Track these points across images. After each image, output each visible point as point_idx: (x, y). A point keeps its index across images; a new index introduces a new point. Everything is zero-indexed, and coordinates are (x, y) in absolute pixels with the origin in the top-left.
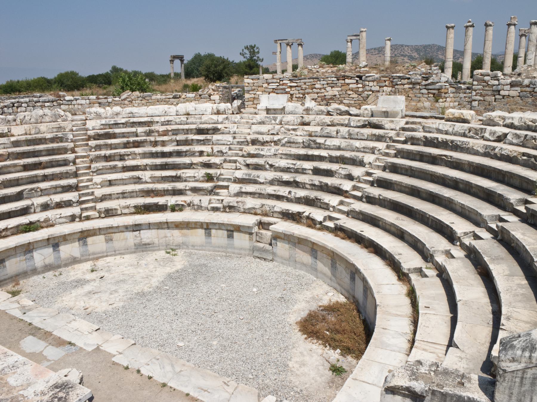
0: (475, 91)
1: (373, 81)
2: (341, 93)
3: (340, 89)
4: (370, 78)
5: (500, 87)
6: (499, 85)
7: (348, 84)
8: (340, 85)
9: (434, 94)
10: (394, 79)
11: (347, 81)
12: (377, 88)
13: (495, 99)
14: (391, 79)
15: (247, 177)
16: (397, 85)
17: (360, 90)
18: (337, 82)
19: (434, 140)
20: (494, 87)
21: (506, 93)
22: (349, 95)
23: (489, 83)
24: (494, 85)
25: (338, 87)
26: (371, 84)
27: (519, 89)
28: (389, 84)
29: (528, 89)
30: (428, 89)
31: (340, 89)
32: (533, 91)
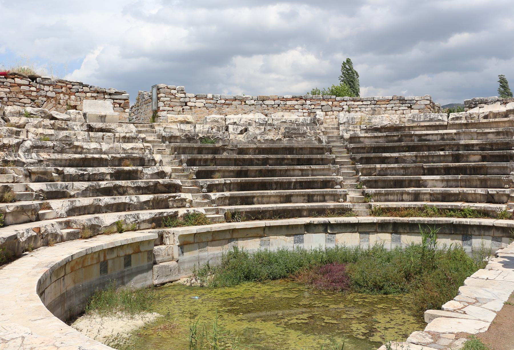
0: (164, 102)
1: (49, 85)
2: (8, 95)
3: (8, 90)
4: (46, 82)
5: (187, 100)
6: (186, 97)
7: (20, 85)
8: (9, 84)
9: (120, 104)
10: (73, 85)
11: (18, 81)
12: (53, 94)
13: (183, 109)
14: (68, 86)
15: (54, 190)
16: (77, 92)
17: (34, 94)
18: (5, 80)
19: (194, 137)
21: (193, 104)
22: (21, 99)
25: (6, 87)
26: (46, 88)
28: (67, 91)
29: (212, 101)
30: (114, 99)
31: (8, 90)
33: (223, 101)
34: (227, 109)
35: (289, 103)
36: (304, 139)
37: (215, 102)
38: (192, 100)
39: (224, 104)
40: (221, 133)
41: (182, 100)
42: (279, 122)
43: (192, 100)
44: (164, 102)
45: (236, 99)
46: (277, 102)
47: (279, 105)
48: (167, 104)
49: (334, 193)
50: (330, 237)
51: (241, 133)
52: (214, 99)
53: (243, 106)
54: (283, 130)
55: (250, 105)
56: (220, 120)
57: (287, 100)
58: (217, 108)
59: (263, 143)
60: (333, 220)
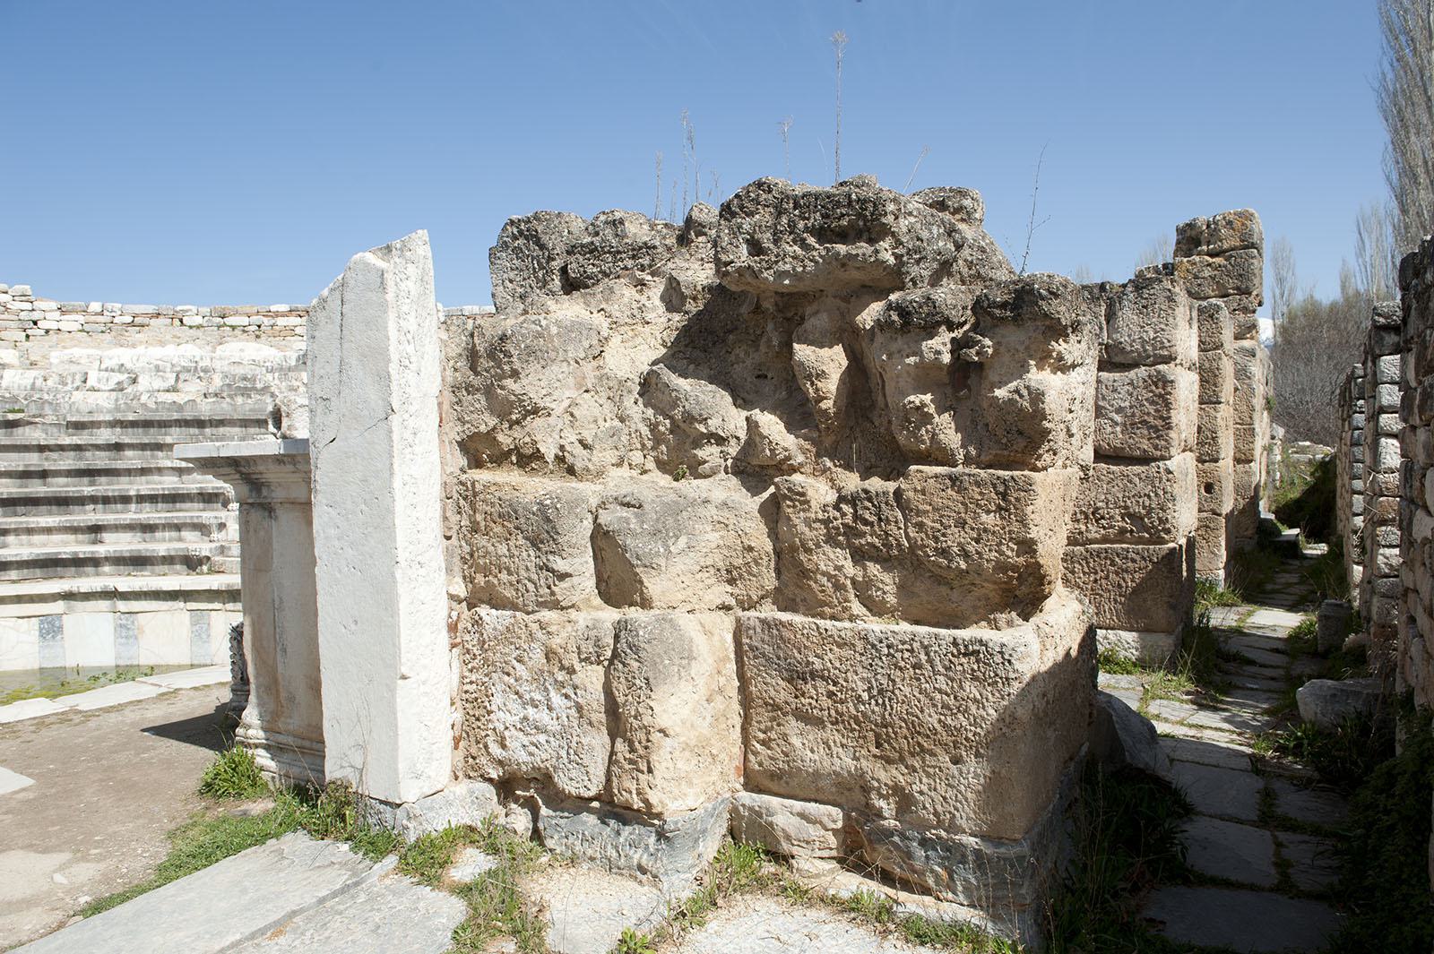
5: (35, 316)
13: (28, 336)
20: (22, 313)
21: (54, 326)
27: (81, 319)
29: (100, 319)
33: (129, 319)
34: (138, 335)
35: (281, 321)
36: (249, 401)
37: (109, 319)
38: (48, 315)
39: (132, 324)
40: (69, 388)
41: (23, 315)
42: (227, 362)
43: (48, 315)
46: (256, 319)
47: (259, 326)
49: (196, 521)
50: (124, 622)
51: (120, 388)
53: (178, 330)
54: (218, 382)
55: (191, 327)
56: (82, 361)
57: (277, 316)
58: (113, 333)
59: (152, 410)
60: (125, 583)
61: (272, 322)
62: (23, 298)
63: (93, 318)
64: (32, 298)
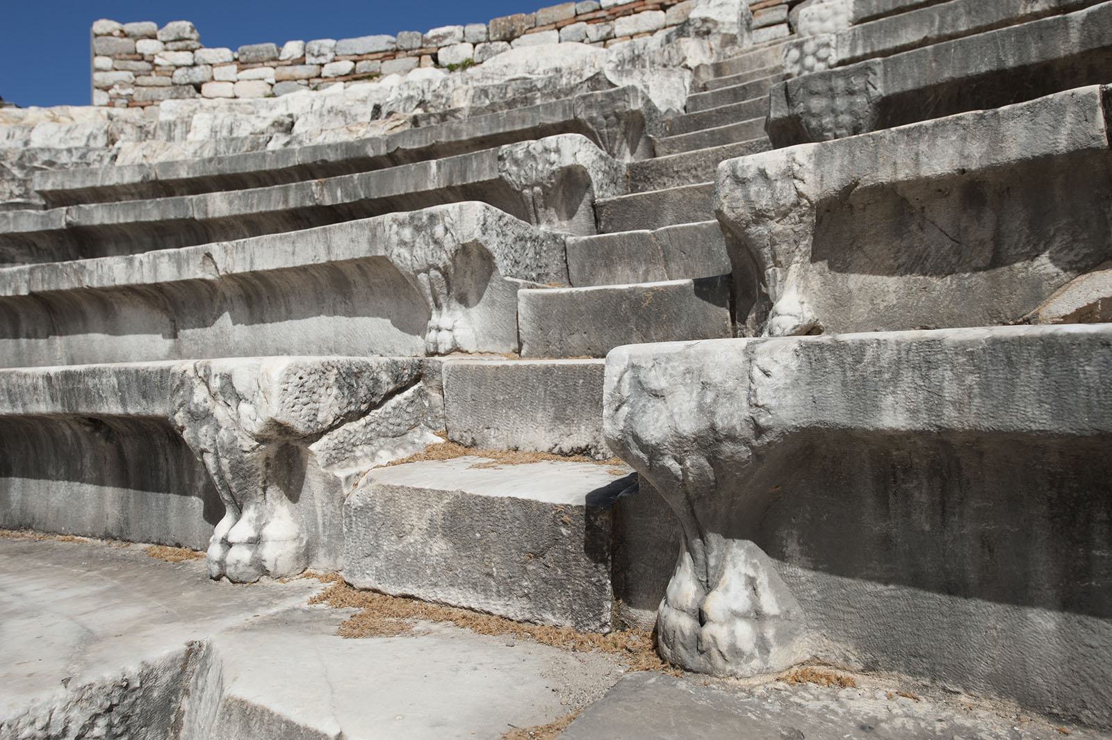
0: (107, 89)
5: (199, 74)
6: (195, 65)
20: (178, 73)
23: (157, 61)
24: (177, 67)
29: (300, 71)
32: (319, 76)
38: (218, 73)
41: (180, 76)
44: (107, 89)
45: (398, 50)
48: (119, 96)
52: (309, 59)
57: (615, 16)
61: (604, 30)
62: (180, 44)
63: (288, 71)
64: (195, 45)
